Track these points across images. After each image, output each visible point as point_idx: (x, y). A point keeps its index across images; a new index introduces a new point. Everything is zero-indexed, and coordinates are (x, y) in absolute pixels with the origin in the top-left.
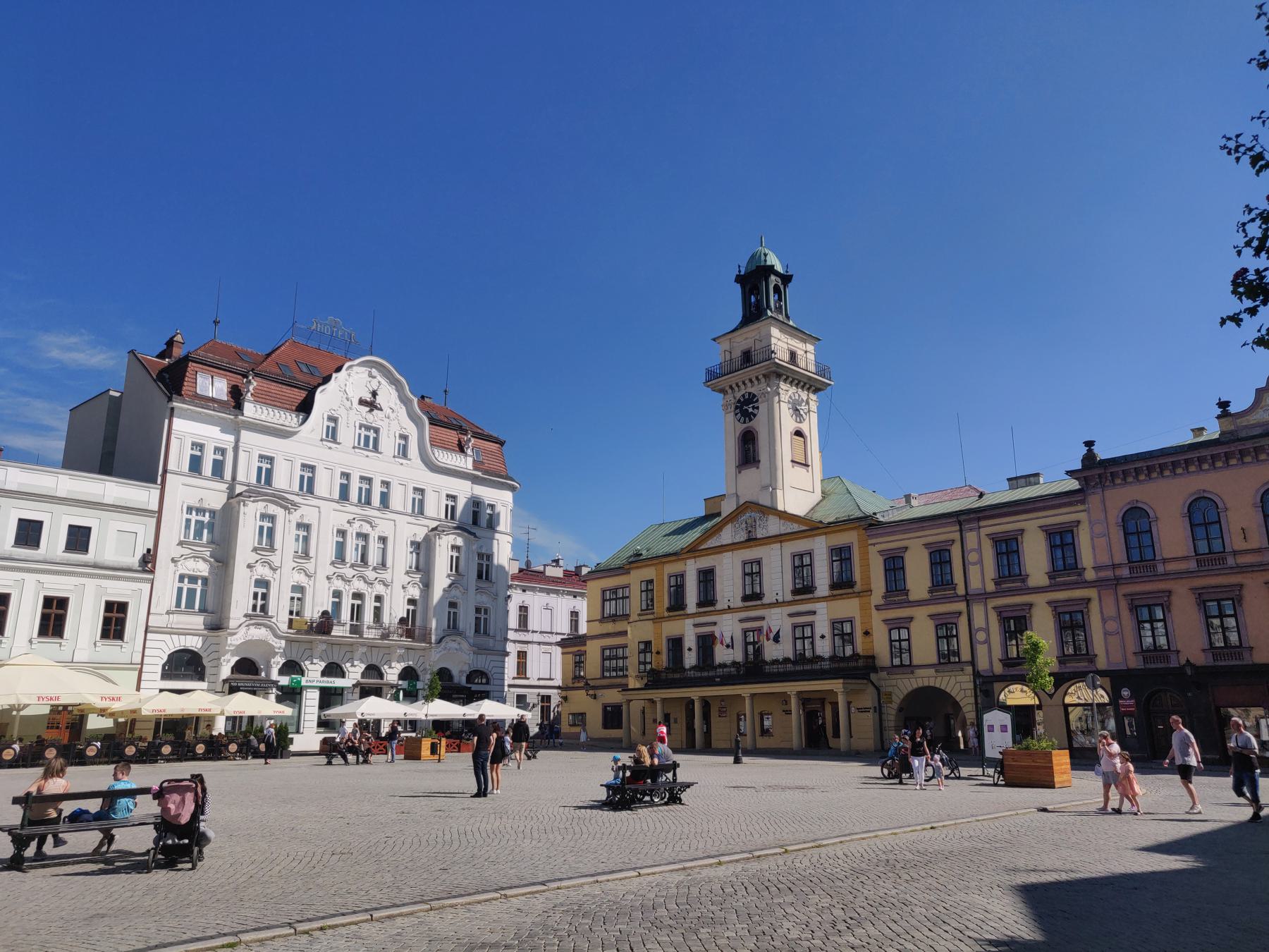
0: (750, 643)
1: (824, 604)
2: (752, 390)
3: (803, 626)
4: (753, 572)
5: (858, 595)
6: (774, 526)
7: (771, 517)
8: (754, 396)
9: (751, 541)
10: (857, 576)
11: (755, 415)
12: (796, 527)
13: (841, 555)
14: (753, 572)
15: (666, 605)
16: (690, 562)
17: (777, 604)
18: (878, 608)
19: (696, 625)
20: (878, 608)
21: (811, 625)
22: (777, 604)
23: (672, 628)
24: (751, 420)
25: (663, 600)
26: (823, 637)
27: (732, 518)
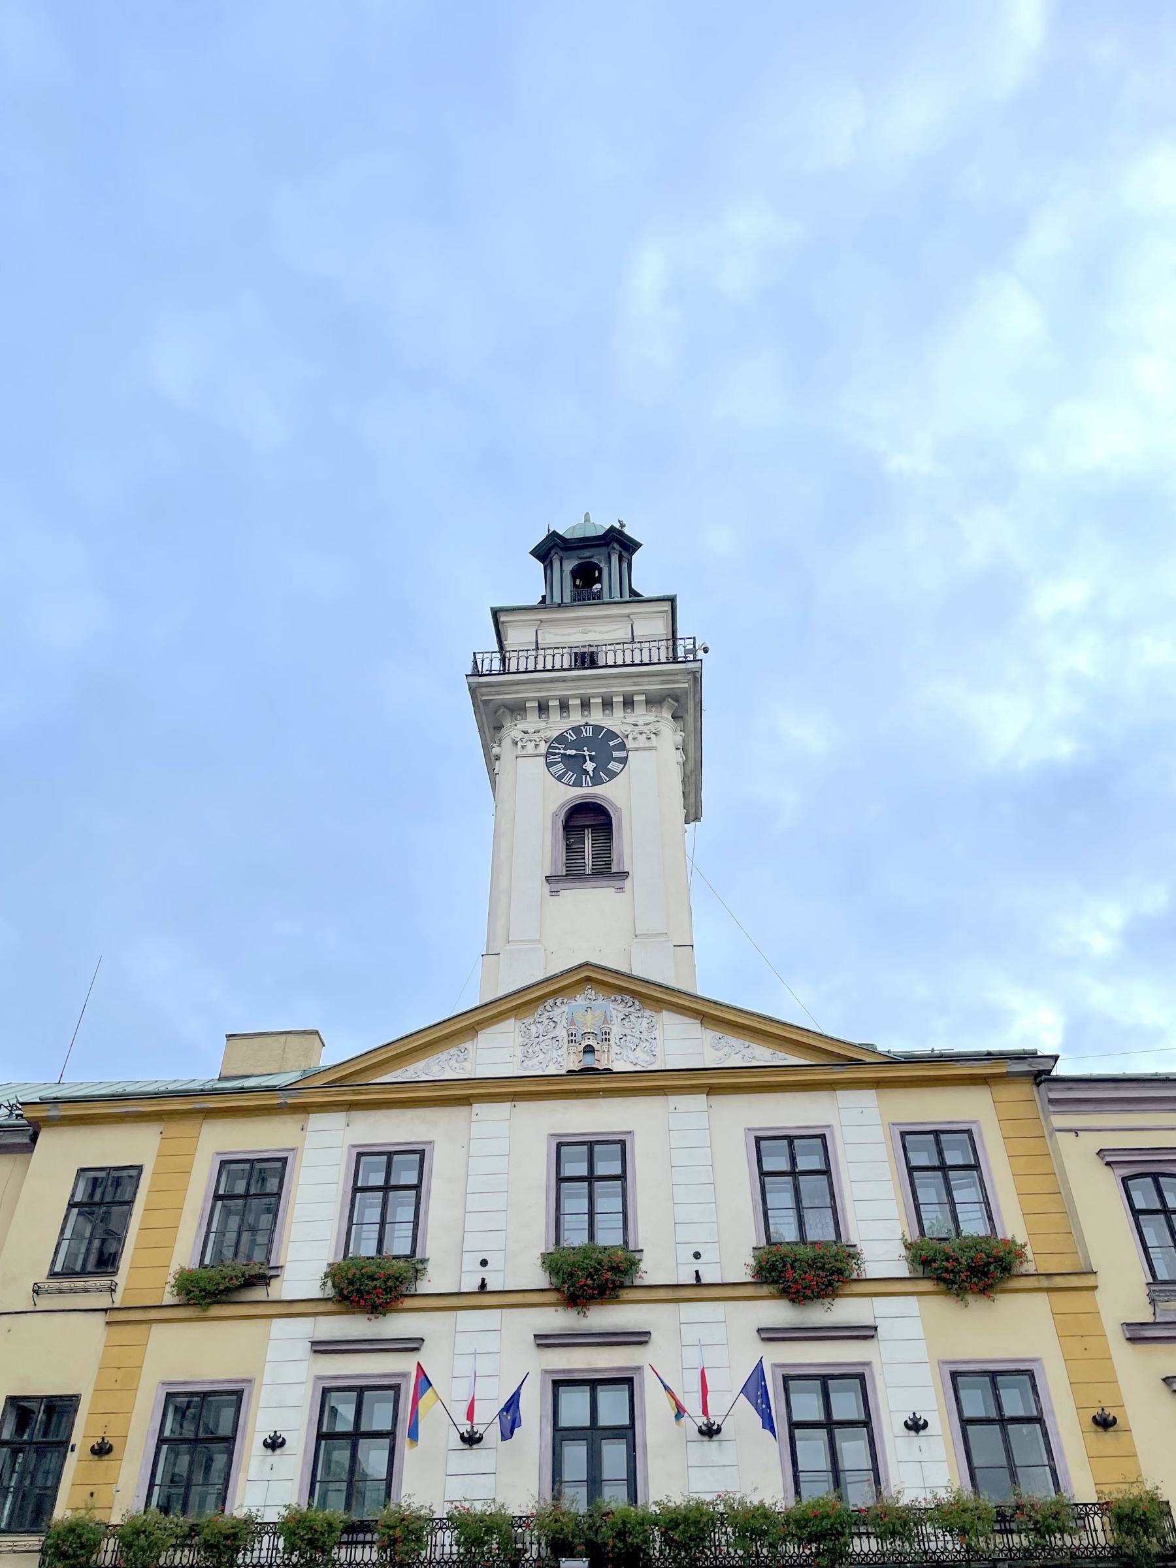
0: (574, 1433)
1: (911, 1305)
2: (615, 721)
3: (825, 1381)
4: (590, 1171)
5: (1049, 1284)
6: (681, 1044)
7: (667, 1017)
8: (612, 735)
9: (588, 1080)
10: (1013, 1226)
11: (612, 775)
12: (763, 1055)
13: (936, 1160)
14: (590, 1171)
15: (185, 1252)
16: (317, 1121)
17: (699, 1289)
18: (1137, 1334)
19: (321, 1348)
20: (1137, 1334)
21: (859, 1378)
22: (699, 1289)
23: (198, 1352)
24: (597, 781)
25: (171, 1234)
26: (916, 1426)
27: (524, 1003)
